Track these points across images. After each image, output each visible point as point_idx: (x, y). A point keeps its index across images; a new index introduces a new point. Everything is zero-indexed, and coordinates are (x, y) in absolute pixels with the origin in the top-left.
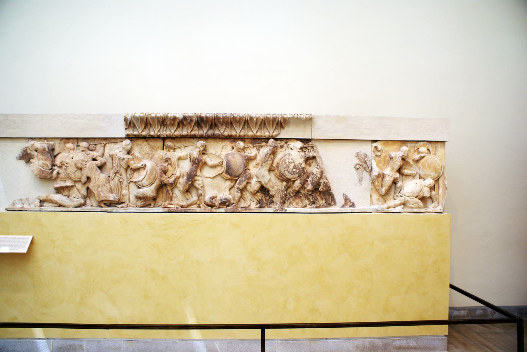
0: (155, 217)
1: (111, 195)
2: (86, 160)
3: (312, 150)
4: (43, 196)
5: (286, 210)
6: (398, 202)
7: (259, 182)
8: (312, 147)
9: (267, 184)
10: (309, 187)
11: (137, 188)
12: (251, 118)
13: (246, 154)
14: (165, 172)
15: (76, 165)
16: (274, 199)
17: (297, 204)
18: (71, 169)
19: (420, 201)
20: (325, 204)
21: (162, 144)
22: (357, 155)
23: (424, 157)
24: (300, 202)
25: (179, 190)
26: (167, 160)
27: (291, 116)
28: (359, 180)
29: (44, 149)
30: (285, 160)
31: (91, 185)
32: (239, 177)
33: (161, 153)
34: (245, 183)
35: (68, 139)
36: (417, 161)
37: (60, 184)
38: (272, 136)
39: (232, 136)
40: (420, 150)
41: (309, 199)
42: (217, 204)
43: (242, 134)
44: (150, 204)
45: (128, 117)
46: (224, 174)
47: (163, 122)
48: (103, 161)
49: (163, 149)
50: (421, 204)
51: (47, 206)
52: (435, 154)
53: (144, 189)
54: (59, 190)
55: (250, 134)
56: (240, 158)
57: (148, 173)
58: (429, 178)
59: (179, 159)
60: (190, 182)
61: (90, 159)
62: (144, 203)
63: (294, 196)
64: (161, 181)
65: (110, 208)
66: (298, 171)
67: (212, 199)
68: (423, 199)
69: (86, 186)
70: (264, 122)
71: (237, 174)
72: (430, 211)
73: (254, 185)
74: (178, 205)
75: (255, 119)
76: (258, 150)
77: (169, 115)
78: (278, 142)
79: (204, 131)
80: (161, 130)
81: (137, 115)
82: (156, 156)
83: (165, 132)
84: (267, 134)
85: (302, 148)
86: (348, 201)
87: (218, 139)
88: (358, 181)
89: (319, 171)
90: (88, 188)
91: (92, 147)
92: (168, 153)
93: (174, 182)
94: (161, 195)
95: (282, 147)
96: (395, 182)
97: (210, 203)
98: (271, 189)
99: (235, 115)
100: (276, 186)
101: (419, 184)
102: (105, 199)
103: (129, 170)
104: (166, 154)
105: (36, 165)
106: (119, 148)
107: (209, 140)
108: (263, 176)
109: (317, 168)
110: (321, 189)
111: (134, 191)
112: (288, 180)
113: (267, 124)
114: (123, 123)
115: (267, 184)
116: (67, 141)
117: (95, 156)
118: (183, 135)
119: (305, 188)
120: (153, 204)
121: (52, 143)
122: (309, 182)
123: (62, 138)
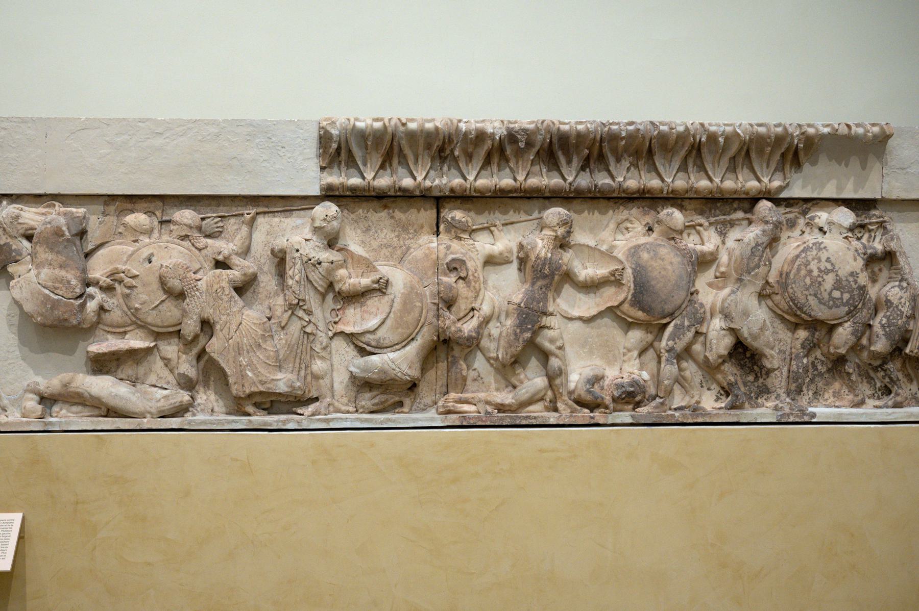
0: (417, 437)
1: (279, 376)
2: (197, 266)
3: (881, 231)
4: (51, 383)
5: (814, 415)
7: (732, 331)
8: (882, 225)
9: (755, 337)
10: (881, 345)
11: (355, 353)
12: (712, 137)
13: (691, 245)
14: (449, 304)
15: (162, 282)
16: (770, 382)
17: (837, 395)
18: (147, 297)
21: (435, 215)
24: (845, 390)
25: (488, 359)
26: (454, 267)
27: (826, 130)
29: (58, 233)
30: (807, 264)
31: (214, 346)
32: (672, 315)
33: (429, 245)
34: (690, 335)
35: (132, 201)
38: (769, 192)
39: (649, 191)
41: (870, 380)
42: (608, 400)
43: (680, 183)
44: (401, 404)
45: (335, 132)
46: (626, 307)
47: (441, 150)
48: (251, 271)
49: (438, 233)
51: (63, 416)
53: (385, 357)
54: (102, 364)
55: (704, 183)
56: (677, 260)
57: (397, 305)
59: (491, 261)
60: (528, 335)
61: (208, 265)
62: (382, 398)
63: (829, 371)
64: (439, 332)
65: (275, 418)
66: (846, 296)
67: (593, 385)
69: (195, 351)
70: (748, 150)
71: (669, 308)
73: (718, 341)
74: (488, 403)
75: (721, 140)
76: (723, 234)
77: (463, 127)
78: (782, 210)
79: (572, 177)
80: (432, 173)
81: (361, 125)
82: (417, 253)
83: (448, 180)
84: (753, 184)
85: (851, 229)
87: (603, 203)
92: (455, 245)
93: (478, 333)
94: (431, 375)
95: (792, 224)
97: (589, 398)
98: (767, 351)
99: (662, 128)
100: (779, 344)
102: (262, 389)
103: (330, 296)
104: (448, 248)
106: (297, 227)
107: (576, 204)
108: (746, 314)
109: (902, 288)
111: (342, 364)
112: (814, 324)
113: (753, 155)
114: (311, 148)
116: (130, 206)
117: (226, 252)
118: (502, 190)
119: (863, 347)
120: (407, 402)
121: (80, 211)
122: (877, 328)
123: (112, 198)
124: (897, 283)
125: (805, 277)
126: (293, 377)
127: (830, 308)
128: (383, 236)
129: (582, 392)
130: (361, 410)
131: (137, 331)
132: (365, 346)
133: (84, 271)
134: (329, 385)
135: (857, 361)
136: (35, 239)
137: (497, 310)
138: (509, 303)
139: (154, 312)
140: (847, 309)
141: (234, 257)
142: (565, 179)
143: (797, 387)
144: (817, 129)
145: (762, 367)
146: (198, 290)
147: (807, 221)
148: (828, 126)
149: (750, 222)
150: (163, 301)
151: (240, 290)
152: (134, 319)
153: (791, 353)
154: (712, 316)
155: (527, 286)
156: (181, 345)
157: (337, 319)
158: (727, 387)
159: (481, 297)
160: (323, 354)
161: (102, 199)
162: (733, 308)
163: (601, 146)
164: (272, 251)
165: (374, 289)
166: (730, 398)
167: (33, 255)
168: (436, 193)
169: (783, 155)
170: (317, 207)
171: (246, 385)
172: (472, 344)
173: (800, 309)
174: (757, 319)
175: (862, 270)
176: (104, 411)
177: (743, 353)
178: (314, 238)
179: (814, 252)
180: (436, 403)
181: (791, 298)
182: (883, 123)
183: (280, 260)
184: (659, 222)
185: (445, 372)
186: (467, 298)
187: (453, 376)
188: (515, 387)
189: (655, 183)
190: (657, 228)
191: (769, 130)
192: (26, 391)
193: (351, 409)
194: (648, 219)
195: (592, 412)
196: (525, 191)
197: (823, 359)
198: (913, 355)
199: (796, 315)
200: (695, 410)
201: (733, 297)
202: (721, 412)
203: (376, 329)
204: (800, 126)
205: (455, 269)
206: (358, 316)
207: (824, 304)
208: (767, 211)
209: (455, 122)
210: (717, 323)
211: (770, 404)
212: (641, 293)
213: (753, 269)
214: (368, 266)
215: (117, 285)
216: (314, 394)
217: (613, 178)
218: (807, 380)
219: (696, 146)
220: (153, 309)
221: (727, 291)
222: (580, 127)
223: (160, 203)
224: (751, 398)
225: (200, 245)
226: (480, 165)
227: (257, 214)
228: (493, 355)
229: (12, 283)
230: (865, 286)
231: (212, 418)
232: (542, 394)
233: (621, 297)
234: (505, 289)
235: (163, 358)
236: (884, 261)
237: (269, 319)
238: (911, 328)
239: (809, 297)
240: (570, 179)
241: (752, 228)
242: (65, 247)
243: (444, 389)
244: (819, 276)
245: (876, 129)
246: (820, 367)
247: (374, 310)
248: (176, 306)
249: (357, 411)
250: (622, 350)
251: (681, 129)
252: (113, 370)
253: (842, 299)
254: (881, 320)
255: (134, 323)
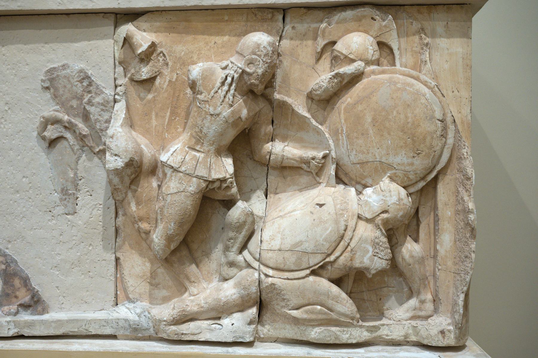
6: (229, 291)
19: (335, 289)
22: (52, 83)
23: (356, 78)
28: (64, 191)
36: (325, 101)
40: (339, 47)
50: (345, 304)
52: (418, 66)
58: (385, 183)
68: (352, 280)
72: (397, 333)
86: (17, 282)
88: (56, 196)
96: (212, 201)
101: (330, 208)
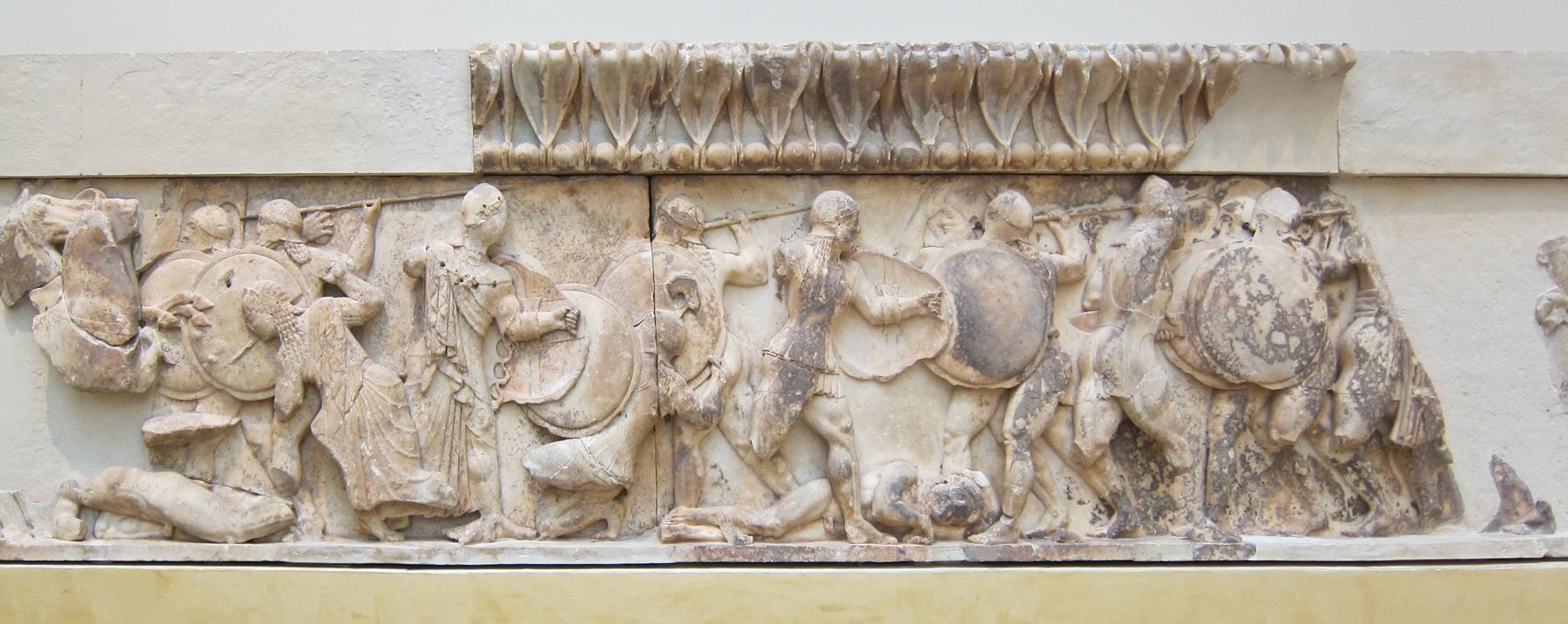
7: (1116, 400)
15: (247, 316)
20: (1412, 513)
25: (735, 448)
29: (98, 238)
32: (1020, 374)
37: (170, 420)
46: (947, 359)
48: (374, 299)
63: (1268, 470)
66: (1295, 342)
71: (1015, 362)
89: (1388, 341)
90: (306, 439)
91: (314, 223)
105: (60, 319)
110: (1402, 432)
112: (1243, 390)
115: (1154, 413)
117: (338, 269)
119: (1322, 431)
122: (1345, 397)
124: (1372, 320)
125: (1227, 308)
126: (440, 476)
127: (1270, 362)
128: (568, 240)
129: (883, 505)
130: (544, 534)
131: (212, 398)
132: (547, 425)
133: (137, 300)
134: (495, 491)
135: (1314, 455)
136: (66, 249)
137: (746, 365)
138: (765, 353)
139: (236, 368)
140: (1295, 364)
141: (349, 276)
142: (844, 143)
143: (1220, 499)
144: (1236, 54)
145: (1163, 463)
146: (297, 331)
147: (1223, 212)
148: (1251, 48)
149: (1134, 214)
150: (248, 349)
151: (360, 330)
152: (208, 379)
153: (1208, 441)
154: (1081, 375)
155: (792, 324)
156: (275, 421)
157: (504, 381)
158: (1109, 499)
159: (721, 343)
160: (485, 438)
161: (161, 185)
162: (1116, 361)
163: (899, 86)
164: (406, 265)
165: (558, 330)
166: (1114, 518)
167: (65, 274)
168: (648, 167)
169: (1182, 99)
170: (470, 193)
171: (371, 489)
172: (711, 421)
173: (1221, 363)
174: (1154, 383)
175: (1317, 297)
176: (167, 530)
177: (1135, 440)
178: (467, 244)
179: (1239, 266)
180: (657, 523)
181: (1205, 344)
182: (1338, 43)
183: (418, 279)
184: (993, 214)
185: (669, 470)
186: (699, 344)
187: (683, 477)
188: (778, 497)
189: (984, 148)
190: (990, 226)
191: (1160, 56)
192: (60, 495)
193: (530, 532)
194: (976, 209)
195: (900, 541)
196: (784, 163)
197: (1258, 450)
198: (1405, 444)
199: (1214, 375)
200: (1063, 539)
201: (1115, 343)
202: (1095, 542)
203: (564, 397)
204: (1207, 49)
205: (681, 295)
206: (536, 376)
207: (1260, 355)
208: (1162, 195)
209: (674, 46)
210: (1091, 390)
211: (1176, 529)
212: (970, 335)
213: (1146, 295)
214: (550, 291)
215: (182, 323)
216: (473, 506)
217: (918, 139)
218: (1236, 486)
219: (1047, 83)
220: (234, 362)
221: (1104, 332)
222: (867, 54)
223: (243, 187)
224: (1147, 518)
225: (300, 257)
226: (714, 119)
227: (382, 205)
228: (741, 442)
229: (36, 319)
230: (1322, 325)
231: (322, 544)
232: (821, 509)
233: (939, 343)
234: (758, 329)
235: (251, 444)
236: (1352, 277)
237: (404, 379)
238: (1396, 397)
239: (1235, 344)
240: (852, 142)
241: (1139, 223)
242: (108, 261)
243: (669, 499)
244: (1249, 306)
245: (1328, 55)
246: (1253, 465)
247: (559, 364)
248: (267, 358)
249: (538, 535)
250: (942, 435)
251: (1023, 55)
252: (180, 462)
253: (1288, 346)
254: (1351, 384)
255: (208, 385)
